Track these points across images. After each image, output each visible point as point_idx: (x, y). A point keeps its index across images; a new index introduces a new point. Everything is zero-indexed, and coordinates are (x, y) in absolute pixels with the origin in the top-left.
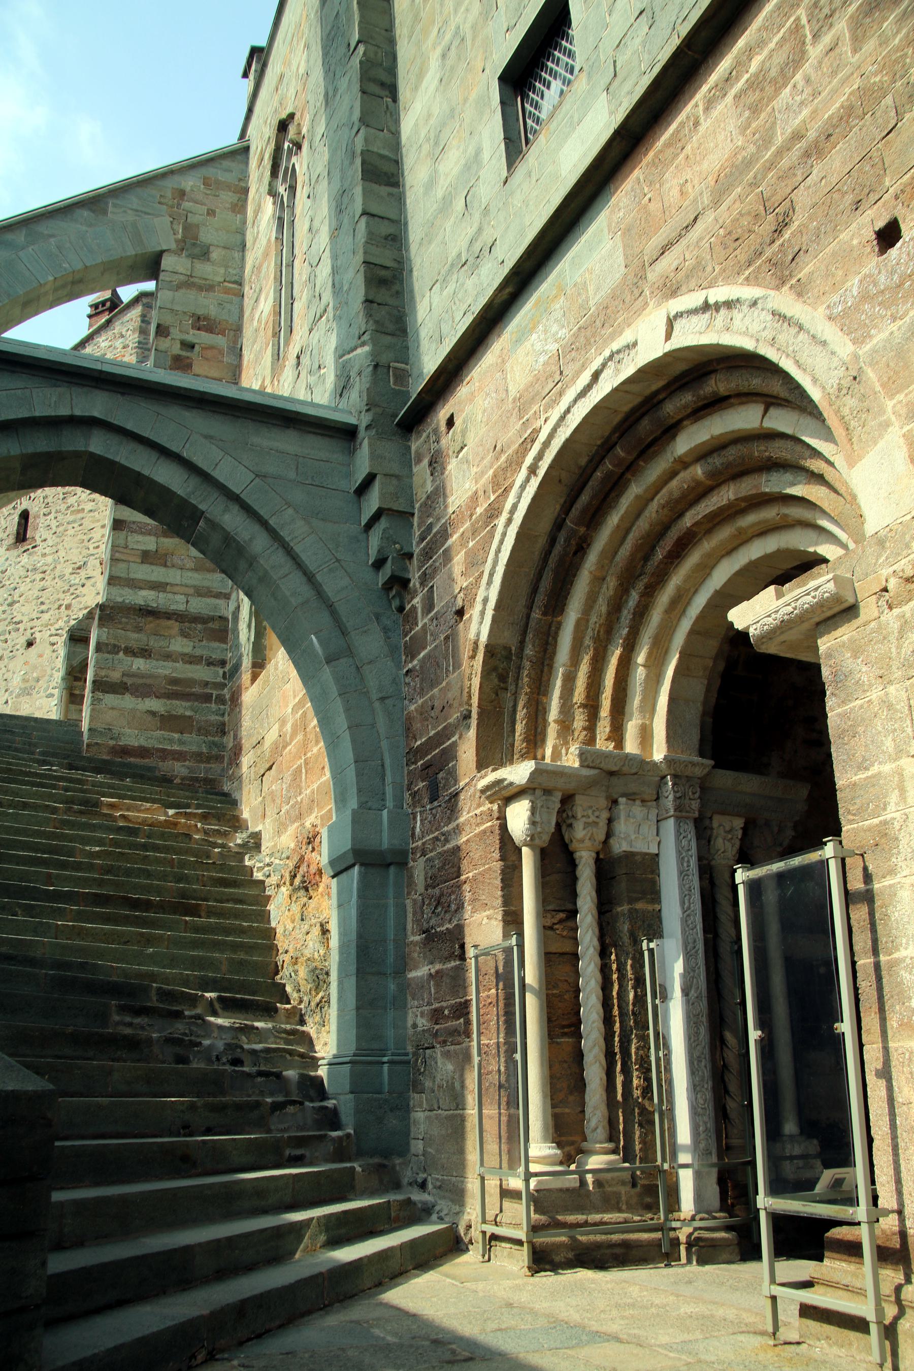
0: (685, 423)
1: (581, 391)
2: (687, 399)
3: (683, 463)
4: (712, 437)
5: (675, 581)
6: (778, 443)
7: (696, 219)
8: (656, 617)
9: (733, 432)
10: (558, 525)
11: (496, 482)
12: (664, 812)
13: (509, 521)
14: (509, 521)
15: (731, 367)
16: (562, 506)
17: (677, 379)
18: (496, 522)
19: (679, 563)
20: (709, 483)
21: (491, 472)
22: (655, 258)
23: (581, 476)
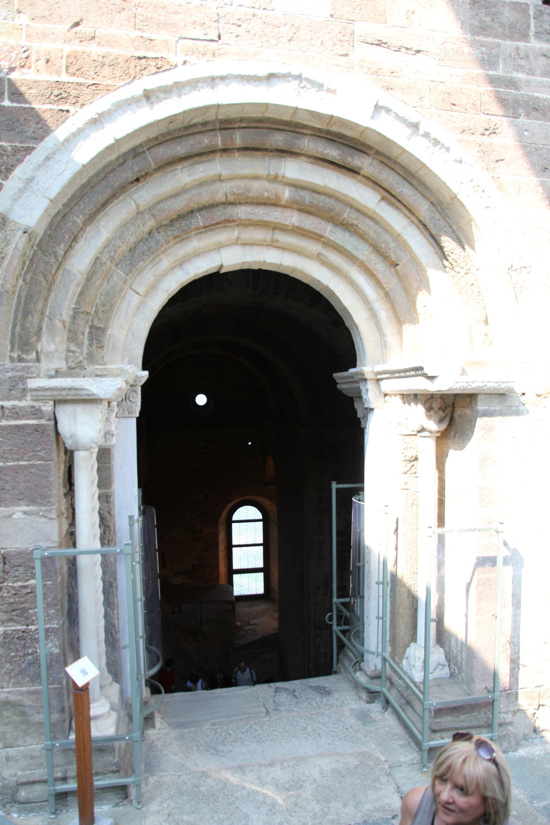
0: (302, 158)
1: (249, 76)
2: (332, 152)
3: (275, 179)
4: (324, 187)
5: (195, 244)
6: (368, 221)
7: (418, 51)
8: (165, 263)
9: (346, 195)
10: (136, 152)
11: (73, 64)
12: (126, 412)
13: (96, 122)
14: (96, 122)
15: (382, 162)
16: (149, 140)
17: (328, 132)
18: (72, 109)
19: (205, 232)
20: (283, 203)
21: (68, 49)
22: (369, 40)
23: (186, 128)
